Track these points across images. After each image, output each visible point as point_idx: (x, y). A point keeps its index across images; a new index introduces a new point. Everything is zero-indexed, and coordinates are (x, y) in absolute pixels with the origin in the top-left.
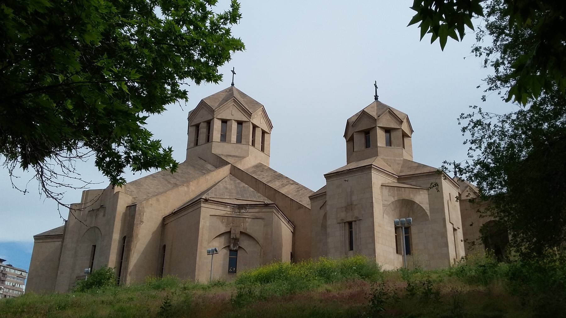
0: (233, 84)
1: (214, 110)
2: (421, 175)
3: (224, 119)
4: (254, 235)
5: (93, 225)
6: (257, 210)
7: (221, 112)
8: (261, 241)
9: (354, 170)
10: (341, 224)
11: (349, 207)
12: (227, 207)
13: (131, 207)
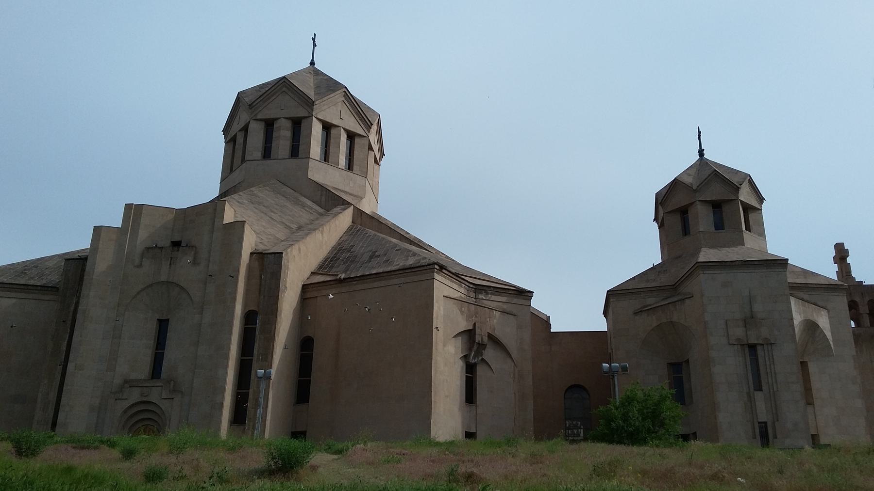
0: (312, 63)
1: (314, 102)
2: (818, 286)
3: (328, 122)
4: (504, 341)
5: (163, 278)
6: (504, 299)
7: (323, 108)
8: (514, 354)
9: (756, 263)
10: (736, 347)
11: (750, 320)
12: (461, 286)
13: (266, 255)
